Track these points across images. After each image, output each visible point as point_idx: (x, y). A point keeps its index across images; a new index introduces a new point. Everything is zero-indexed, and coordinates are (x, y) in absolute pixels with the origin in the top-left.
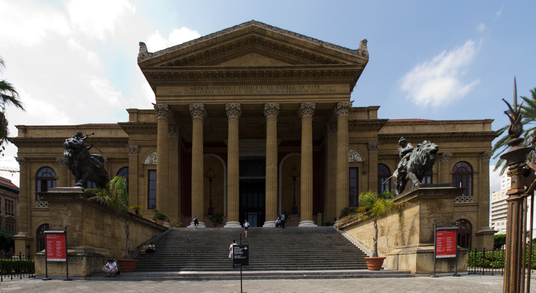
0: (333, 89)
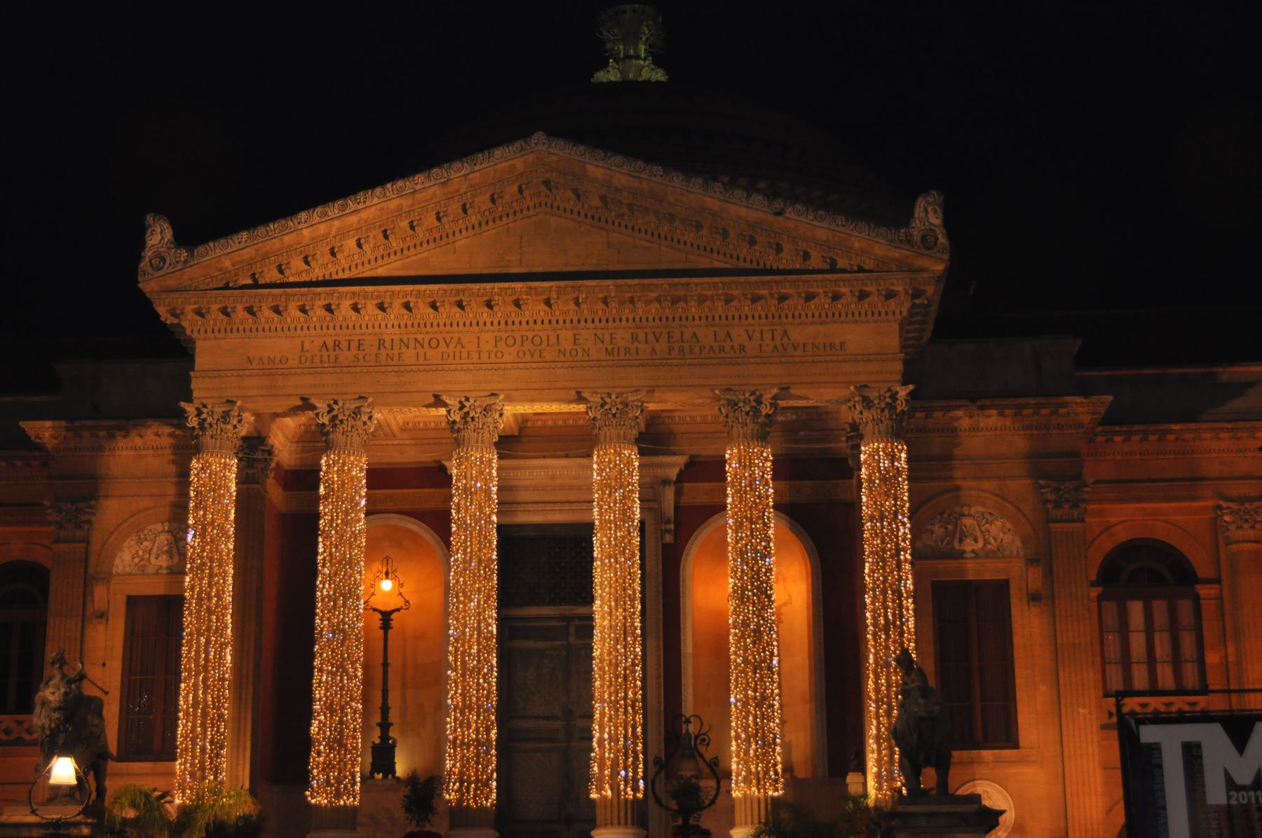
0: (837, 342)
